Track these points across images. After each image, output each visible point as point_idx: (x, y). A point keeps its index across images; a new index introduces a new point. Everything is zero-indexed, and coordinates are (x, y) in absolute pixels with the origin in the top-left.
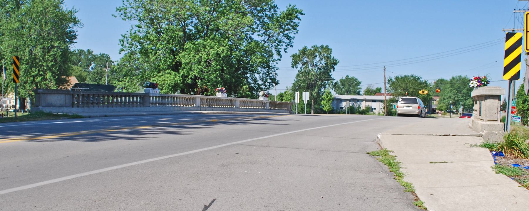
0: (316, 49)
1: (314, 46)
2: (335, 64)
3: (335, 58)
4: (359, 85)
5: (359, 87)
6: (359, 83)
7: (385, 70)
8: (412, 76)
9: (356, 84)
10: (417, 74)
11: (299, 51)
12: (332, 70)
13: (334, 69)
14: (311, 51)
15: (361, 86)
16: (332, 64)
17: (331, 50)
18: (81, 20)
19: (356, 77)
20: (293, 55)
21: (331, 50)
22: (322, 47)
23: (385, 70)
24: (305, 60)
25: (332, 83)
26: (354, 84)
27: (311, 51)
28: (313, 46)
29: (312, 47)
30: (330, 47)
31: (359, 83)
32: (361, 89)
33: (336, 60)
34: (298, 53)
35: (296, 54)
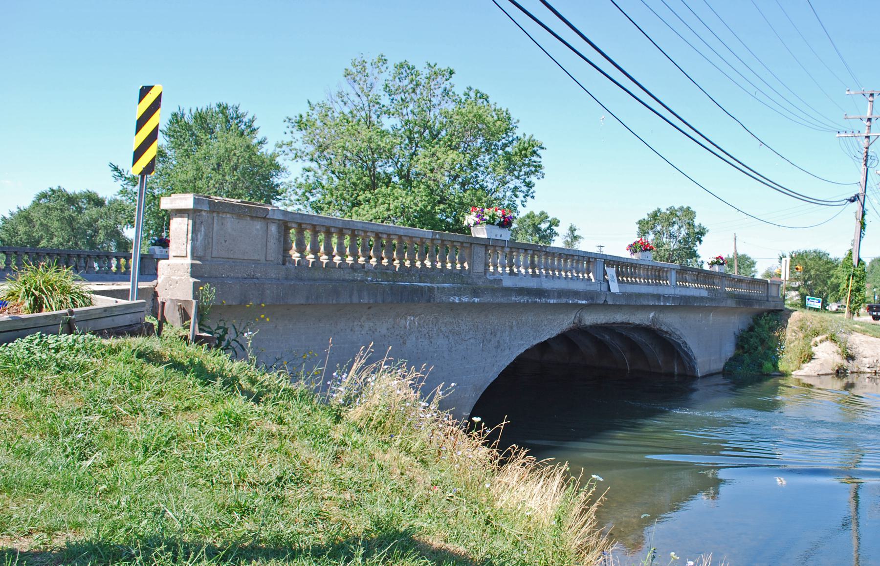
0: (673, 212)
1: (671, 208)
2: (702, 234)
3: (702, 225)
4: (754, 267)
5: (753, 269)
6: (753, 263)
7: (735, 239)
8: (815, 252)
9: (748, 266)
10: (822, 248)
11: (648, 215)
12: (698, 243)
13: (700, 241)
14: (664, 215)
15: (757, 266)
16: (699, 235)
17: (695, 213)
18: (288, 167)
19: (749, 255)
20: (640, 221)
21: (695, 213)
22: (681, 209)
23: (735, 239)
24: (659, 228)
25: (696, 261)
26: (745, 266)
27: (664, 215)
28: (668, 207)
29: (667, 209)
30: (693, 209)
31: (753, 263)
32: (756, 272)
33: (704, 229)
34: (646, 217)
35: (644, 219)
